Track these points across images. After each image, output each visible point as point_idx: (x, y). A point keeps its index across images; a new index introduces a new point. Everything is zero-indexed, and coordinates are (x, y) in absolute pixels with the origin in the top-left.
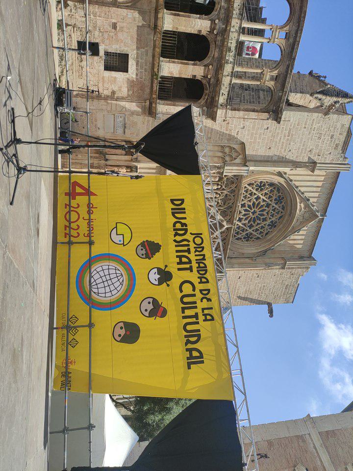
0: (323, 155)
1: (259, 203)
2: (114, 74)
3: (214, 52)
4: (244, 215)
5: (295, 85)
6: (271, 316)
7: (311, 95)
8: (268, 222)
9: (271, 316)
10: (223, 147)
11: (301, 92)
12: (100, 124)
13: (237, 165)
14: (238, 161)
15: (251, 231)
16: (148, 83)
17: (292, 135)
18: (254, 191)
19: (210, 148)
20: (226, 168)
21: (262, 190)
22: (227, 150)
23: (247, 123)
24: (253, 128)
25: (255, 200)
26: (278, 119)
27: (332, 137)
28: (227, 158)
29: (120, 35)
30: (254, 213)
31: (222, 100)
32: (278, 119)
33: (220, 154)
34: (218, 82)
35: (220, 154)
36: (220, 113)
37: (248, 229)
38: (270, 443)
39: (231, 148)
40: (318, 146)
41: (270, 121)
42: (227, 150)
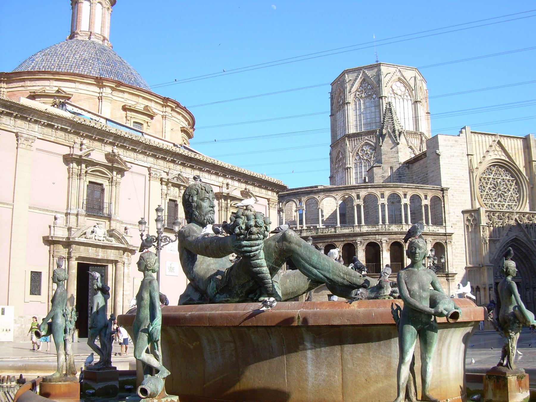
0: (462, 150)
1: (493, 187)
4: (501, 197)
5: (392, 158)
7: (398, 144)
11: (398, 153)
15: (511, 190)
17: (454, 177)
18: (485, 193)
20: (482, 224)
21: (484, 187)
23: (451, 211)
24: (453, 206)
25: (491, 191)
26: (447, 189)
27: (452, 146)
31: (441, 231)
32: (447, 189)
37: (510, 193)
40: (458, 156)
41: (448, 194)
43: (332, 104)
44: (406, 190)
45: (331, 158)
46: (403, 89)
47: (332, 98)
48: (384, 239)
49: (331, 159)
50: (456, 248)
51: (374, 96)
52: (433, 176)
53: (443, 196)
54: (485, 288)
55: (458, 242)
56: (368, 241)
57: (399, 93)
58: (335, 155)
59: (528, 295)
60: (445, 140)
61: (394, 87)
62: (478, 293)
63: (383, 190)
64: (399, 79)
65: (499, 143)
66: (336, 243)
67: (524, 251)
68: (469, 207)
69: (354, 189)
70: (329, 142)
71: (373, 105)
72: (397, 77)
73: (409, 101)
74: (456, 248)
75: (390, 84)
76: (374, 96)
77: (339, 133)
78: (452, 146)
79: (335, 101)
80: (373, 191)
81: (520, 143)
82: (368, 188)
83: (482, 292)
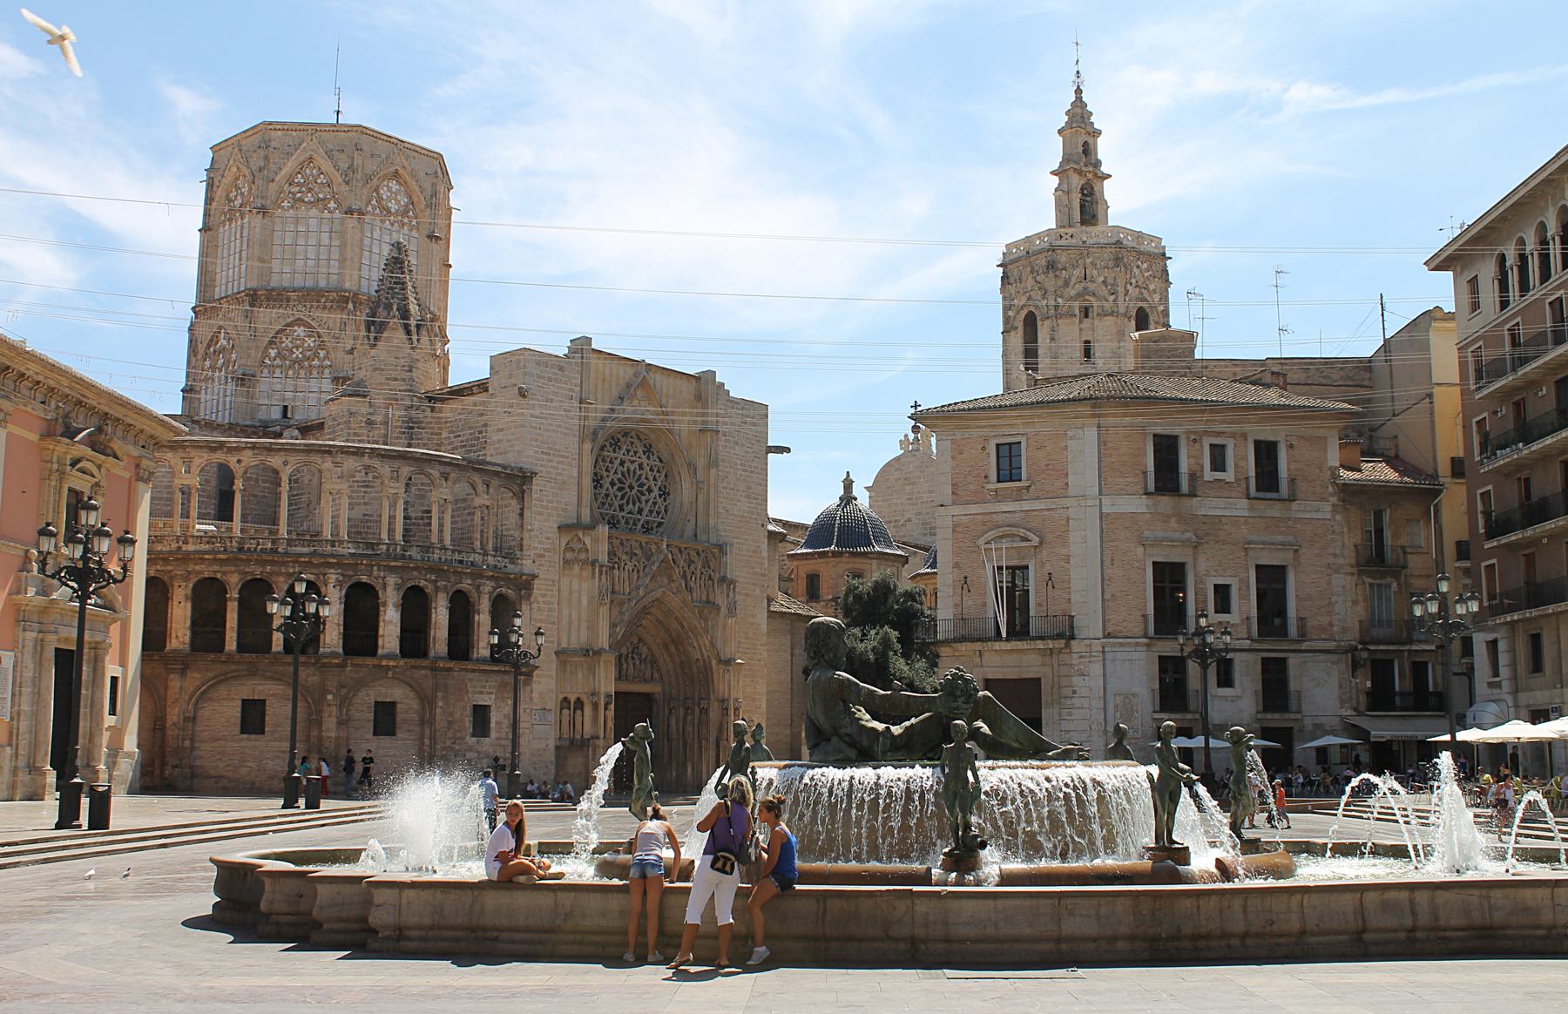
2: (493, 725)
3: (466, 585)
6: (788, 450)
8: (645, 461)
9: (788, 450)
10: (567, 562)
12: (543, 746)
13: (596, 540)
14: (588, 541)
15: (656, 490)
16: (499, 678)
19: (565, 582)
22: (569, 555)
24: (541, 514)
27: (550, 380)
28: (583, 556)
29: (457, 716)
30: (631, 488)
33: (576, 568)
34: (499, 576)
35: (576, 568)
36: (527, 566)
38: (956, 565)
39: (568, 548)
42: (569, 555)
43: (209, 200)
44: (448, 469)
45: (191, 341)
46: (404, 200)
47: (210, 185)
48: (392, 580)
49: (192, 343)
50: (539, 609)
51: (332, 205)
52: (500, 441)
53: (523, 492)
54: (595, 706)
55: (544, 596)
56: (355, 579)
57: (393, 206)
58: (205, 333)
59: (673, 723)
60: (538, 363)
61: (384, 192)
62: (579, 712)
63: (396, 464)
64: (396, 175)
65: (644, 383)
66: (274, 578)
67: (675, 625)
68: (569, 521)
69: (329, 452)
70: (189, 296)
71: (325, 228)
72: (392, 169)
73: (414, 233)
74: (539, 609)
75: (375, 182)
76: (332, 205)
77: (221, 278)
78: (550, 380)
79: (219, 193)
80: (376, 463)
81: (687, 389)
82: (363, 455)
83: (588, 710)
